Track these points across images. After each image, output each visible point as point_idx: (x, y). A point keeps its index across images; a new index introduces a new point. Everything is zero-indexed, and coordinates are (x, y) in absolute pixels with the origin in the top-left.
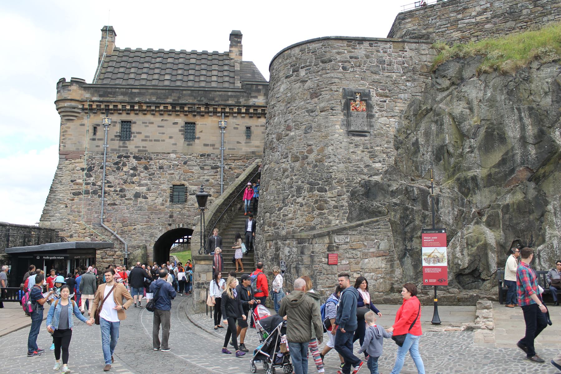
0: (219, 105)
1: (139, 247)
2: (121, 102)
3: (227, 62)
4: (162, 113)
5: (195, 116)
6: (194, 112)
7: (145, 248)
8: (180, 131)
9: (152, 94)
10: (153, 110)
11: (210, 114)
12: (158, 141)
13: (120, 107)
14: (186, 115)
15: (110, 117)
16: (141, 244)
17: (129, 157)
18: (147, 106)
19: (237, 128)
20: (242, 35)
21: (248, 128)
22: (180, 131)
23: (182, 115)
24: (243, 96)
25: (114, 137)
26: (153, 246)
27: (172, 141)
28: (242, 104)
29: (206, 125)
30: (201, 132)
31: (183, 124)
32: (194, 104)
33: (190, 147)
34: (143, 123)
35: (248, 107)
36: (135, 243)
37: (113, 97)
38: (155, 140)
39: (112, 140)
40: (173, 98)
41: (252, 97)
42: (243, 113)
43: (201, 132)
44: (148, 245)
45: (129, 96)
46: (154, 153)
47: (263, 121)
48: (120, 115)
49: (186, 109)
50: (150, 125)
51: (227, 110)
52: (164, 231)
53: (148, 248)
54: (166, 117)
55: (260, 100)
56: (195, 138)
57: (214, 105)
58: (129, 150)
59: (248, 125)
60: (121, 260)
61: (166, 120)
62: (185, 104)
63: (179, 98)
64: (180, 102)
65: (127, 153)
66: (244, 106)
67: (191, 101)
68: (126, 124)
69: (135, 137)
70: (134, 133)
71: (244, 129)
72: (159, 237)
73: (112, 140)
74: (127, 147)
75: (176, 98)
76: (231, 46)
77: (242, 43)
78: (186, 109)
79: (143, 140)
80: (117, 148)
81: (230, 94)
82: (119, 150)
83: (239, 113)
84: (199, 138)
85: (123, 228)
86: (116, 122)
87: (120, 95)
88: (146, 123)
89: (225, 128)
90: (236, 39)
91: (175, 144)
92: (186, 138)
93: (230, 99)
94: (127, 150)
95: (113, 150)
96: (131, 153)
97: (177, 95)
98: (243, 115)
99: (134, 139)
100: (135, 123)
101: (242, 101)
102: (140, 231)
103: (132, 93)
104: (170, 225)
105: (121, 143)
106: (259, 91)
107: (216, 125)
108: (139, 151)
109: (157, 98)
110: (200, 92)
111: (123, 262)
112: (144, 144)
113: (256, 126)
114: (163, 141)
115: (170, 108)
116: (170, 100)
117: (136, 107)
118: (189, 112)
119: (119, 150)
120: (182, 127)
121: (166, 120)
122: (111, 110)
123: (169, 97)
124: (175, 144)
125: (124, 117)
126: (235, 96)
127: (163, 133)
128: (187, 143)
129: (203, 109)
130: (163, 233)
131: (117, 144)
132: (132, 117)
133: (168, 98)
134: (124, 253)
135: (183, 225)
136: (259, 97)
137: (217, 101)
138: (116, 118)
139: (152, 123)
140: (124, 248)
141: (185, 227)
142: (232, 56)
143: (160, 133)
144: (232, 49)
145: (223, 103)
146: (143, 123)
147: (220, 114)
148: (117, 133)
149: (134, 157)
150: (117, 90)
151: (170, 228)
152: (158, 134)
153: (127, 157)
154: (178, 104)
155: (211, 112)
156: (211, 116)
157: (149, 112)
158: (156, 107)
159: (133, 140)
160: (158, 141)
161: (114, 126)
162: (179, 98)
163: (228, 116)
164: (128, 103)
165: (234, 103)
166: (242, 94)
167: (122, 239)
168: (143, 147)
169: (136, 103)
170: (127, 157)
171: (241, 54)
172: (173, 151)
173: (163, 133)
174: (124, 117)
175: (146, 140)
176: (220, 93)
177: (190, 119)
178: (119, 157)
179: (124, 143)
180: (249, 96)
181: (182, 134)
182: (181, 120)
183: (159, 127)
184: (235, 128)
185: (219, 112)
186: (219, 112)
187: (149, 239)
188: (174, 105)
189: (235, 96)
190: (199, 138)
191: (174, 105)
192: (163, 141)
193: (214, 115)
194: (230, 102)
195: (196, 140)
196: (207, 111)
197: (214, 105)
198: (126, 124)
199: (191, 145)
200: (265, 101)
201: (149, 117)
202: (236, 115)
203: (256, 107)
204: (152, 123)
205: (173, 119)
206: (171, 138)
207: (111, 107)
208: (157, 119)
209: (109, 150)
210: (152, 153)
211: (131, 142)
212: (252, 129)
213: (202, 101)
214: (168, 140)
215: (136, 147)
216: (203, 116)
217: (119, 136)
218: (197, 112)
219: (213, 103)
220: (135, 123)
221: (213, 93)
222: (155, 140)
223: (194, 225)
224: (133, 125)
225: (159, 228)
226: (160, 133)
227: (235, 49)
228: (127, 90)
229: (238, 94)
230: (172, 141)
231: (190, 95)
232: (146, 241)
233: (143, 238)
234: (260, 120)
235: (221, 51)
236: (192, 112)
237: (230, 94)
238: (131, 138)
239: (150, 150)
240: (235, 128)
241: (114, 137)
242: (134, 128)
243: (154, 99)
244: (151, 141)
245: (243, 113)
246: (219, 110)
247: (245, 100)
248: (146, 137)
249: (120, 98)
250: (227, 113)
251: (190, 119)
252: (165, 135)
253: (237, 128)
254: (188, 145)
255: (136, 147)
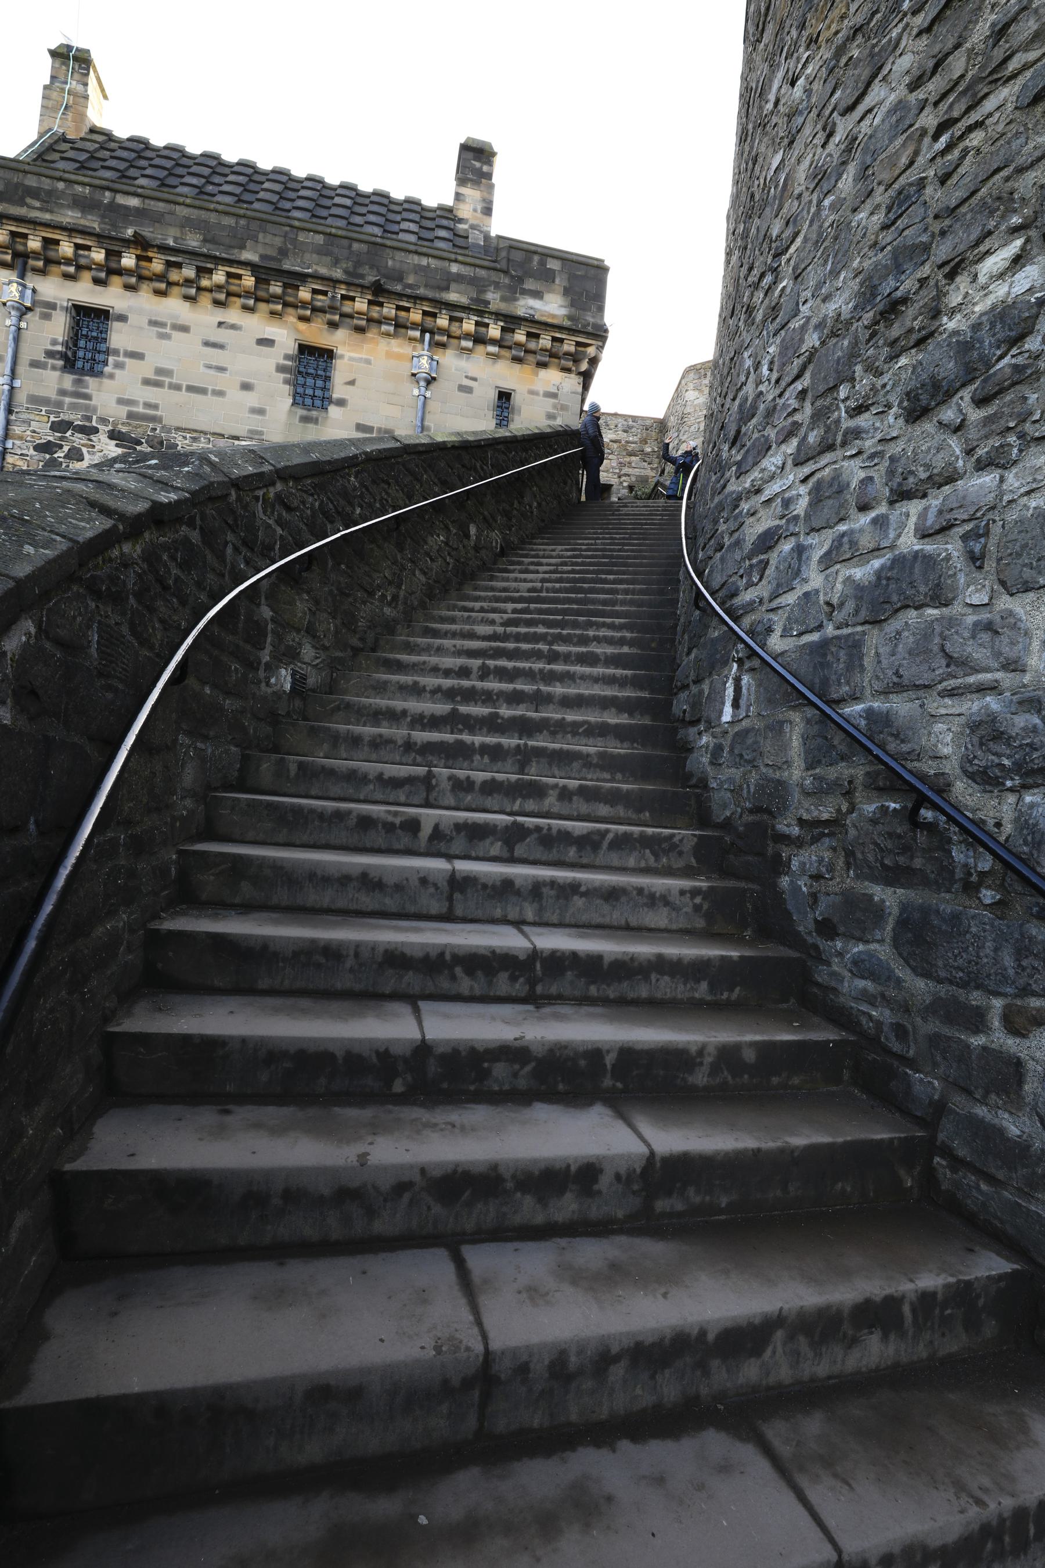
0: (416, 299)
2: (71, 231)
3: (445, 222)
4: (222, 297)
5: (333, 325)
6: (333, 309)
8: (281, 369)
9: (187, 224)
10: (188, 282)
11: (384, 328)
12: (202, 391)
13: (66, 249)
14: (302, 319)
15: (33, 281)
17: (96, 431)
18: (169, 264)
19: (468, 390)
20: (493, 154)
21: (504, 396)
22: (281, 369)
23: (291, 318)
24: (497, 285)
25: (41, 357)
27: (251, 399)
28: (492, 307)
29: (368, 362)
30: (352, 383)
31: (292, 348)
32: (335, 282)
33: (310, 426)
34: (153, 323)
35: (511, 322)
37: (40, 209)
38: (191, 389)
39: (35, 364)
40: (261, 250)
41: (525, 292)
42: (493, 342)
43: (352, 383)
45: (103, 217)
46: (185, 430)
47: (552, 377)
48: (69, 284)
49: (304, 294)
50: (176, 335)
51: (443, 322)
54: (233, 315)
55: (552, 306)
56: (330, 400)
57: (401, 296)
58: (95, 410)
59: (506, 385)
61: (233, 327)
62: (303, 278)
63: (283, 252)
64: (287, 266)
65: (89, 419)
66: (498, 316)
67: (323, 271)
68: (90, 321)
69: (119, 366)
70: (116, 352)
71: (493, 395)
73: (35, 364)
74: (88, 397)
75: (272, 252)
76: (461, 181)
77: (495, 180)
78: (304, 294)
79: (147, 382)
80: (53, 395)
81: (454, 268)
82: (59, 404)
83: (479, 340)
84: (341, 403)
86: (52, 306)
87: (69, 207)
88: (162, 325)
89: (430, 381)
90: (478, 164)
91: (261, 412)
92: (299, 399)
93: (453, 286)
94: (87, 408)
95: (36, 400)
96: (103, 421)
97: (278, 241)
98: (492, 349)
99: (117, 372)
100: (122, 318)
101: (494, 299)
103: (113, 207)
105: (68, 381)
106: (548, 277)
107: (406, 369)
108: (131, 416)
109: (205, 241)
110: (356, 246)
112: (151, 394)
113: (532, 392)
114: (220, 393)
115: (249, 281)
116: (247, 255)
117: (128, 261)
118: (314, 310)
119: (59, 404)
120: (287, 357)
121: (233, 327)
122: (36, 255)
123: (249, 243)
124: (261, 412)
125: (85, 292)
126: (473, 281)
127: (222, 369)
128: (300, 412)
129: (361, 305)
131: (52, 381)
132: (111, 297)
133: (242, 247)
136: (548, 297)
137: (410, 286)
138: (52, 288)
139: (185, 329)
142: (465, 211)
143: (209, 367)
144: (464, 190)
145: (430, 294)
146: (153, 323)
147: (417, 334)
148: (54, 342)
149: (113, 435)
150: (61, 185)
152: (202, 369)
153: (89, 431)
154: (280, 273)
155: (386, 320)
156: (388, 334)
157: (176, 290)
158: (201, 271)
159: (111, 376)
160: (202, 391)
161: (46, 317)
162: (283, 252)
163: (443, 346)
164: (100, 237)
165: (464, 300)
166: (494, 276)
168: (147, 405)
169: (127, 243)
170: (89, 431)
171: (488, 211)
172: (251, 431)
173: (222, 369)
174: (85, 292)
175: (158, 384)
176: (424, 261)
177: (317, 334)
178: (55, 427)
179: (78, 382)
180: (515, 289)
181: (286, 382)
182: (287, 335)
183: (207, 344)
184: (463, 389)
185: (415, 326)
186: (415, 326)
188: (263, 273)
189: (473, 281)
190: (341, 403)
191: (263, 273)
192: (220, 393)
193: (395, 335)
194: (453, 297)
195: (333, 410)
196: (375, 315)
197: (401, 296)
198: (90, 321)
199: (316, 421)
200: (563, 312)
201: (174, 306)
202: (469, 344)
203: (536, 326)
204: (185, 329)
205: (257, 324)
206: (246, 387)
207: (34, 244)
208: (203, 317)
209: (21, 398)
210: (178, 429)
211: (106, 381)
212: (517, 399)
213: (362, 276)
214: (235, 394)
215: (121, 401)
216: (360, 330)
217: (63, 356)
218: (342, 315)
219: (398, 288)
220: (122, 318)
221: (400, 256)
222: (191, 389)
224: (116, 325)
226: (209, 367)
227: (471, 193)
228: (97, 195)
229: (483, 273)
230: (251, 399)
231: (321, 251)
234: (543, 373)
235: (430, 200)
236: (322, 310)
237: (454, 268)
238: (107, 369)
239: (170, 418)
240: (463, 389)
241: (41, 357)
242: (119, 337)
243: (193, 242)
244: (177, 387)
245: (493, 342)
246: (416, 316)
247: (503, 299)
248: (160, 371)
249: (70, 216)
250: (442, 331)
251: (317, 334)
252: (227, 375)
253: (468, 390)
254: (305, 419)
255: (121, 401)
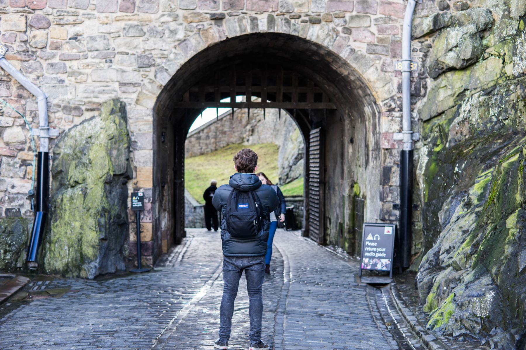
1: (95, 108)
7: (120, 110)
16: (103, 98)
26: (151, 103)
36: (74, 93)
44: (129, 98)
52: (197, 45)
53: (132, 111)
60: (24, 163)
72: (173, 70)
85: (31, 34)
102: (100, 44)
104: (218, 19)
111: (32, 170)
130: (191, 54)
134: (36, 132)
135: (271, 21)
140: (35, 116)
141: (280, 28)
151: (217, 34)
167: (27, 80)
187: (133, 77)
223: (315, 21)
225: (173, 32)
232: (122, 84)
233: (112, 75)
